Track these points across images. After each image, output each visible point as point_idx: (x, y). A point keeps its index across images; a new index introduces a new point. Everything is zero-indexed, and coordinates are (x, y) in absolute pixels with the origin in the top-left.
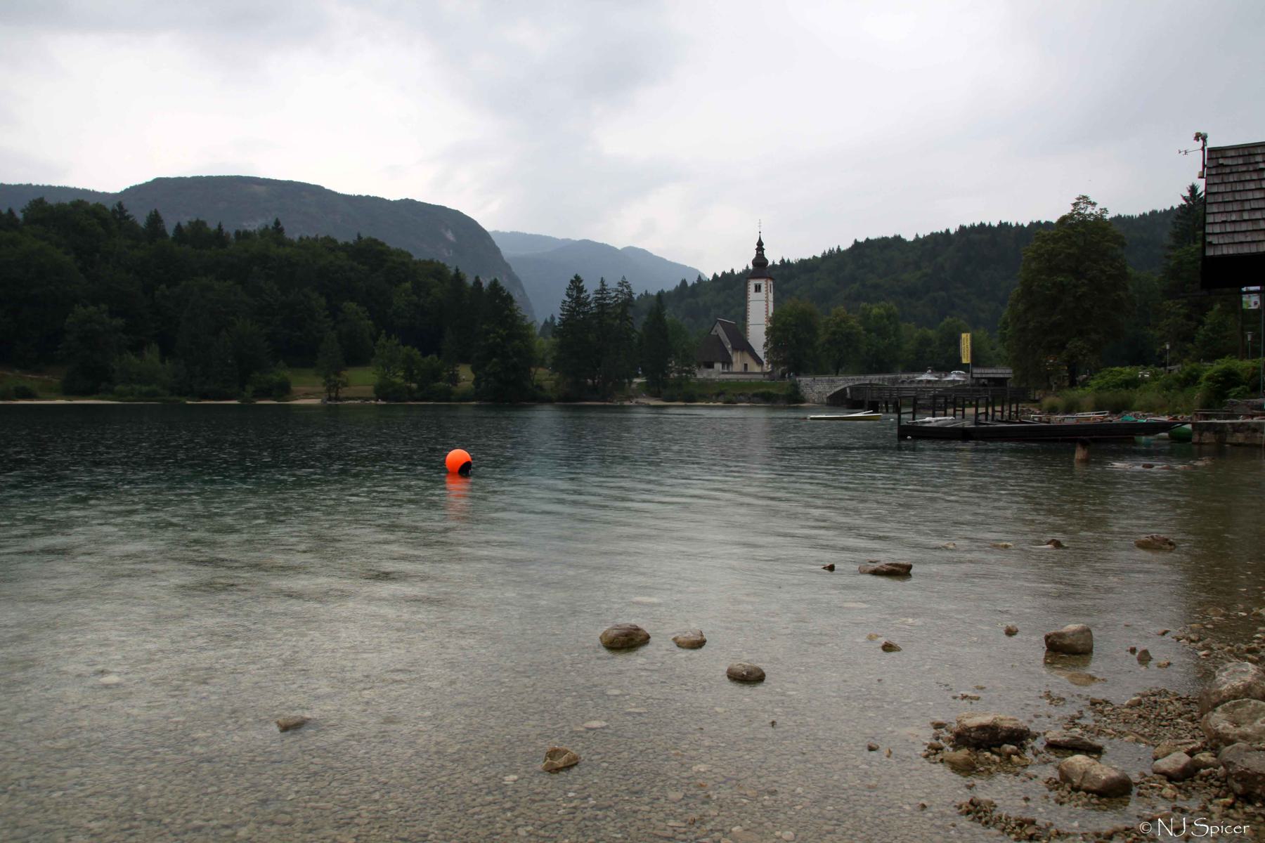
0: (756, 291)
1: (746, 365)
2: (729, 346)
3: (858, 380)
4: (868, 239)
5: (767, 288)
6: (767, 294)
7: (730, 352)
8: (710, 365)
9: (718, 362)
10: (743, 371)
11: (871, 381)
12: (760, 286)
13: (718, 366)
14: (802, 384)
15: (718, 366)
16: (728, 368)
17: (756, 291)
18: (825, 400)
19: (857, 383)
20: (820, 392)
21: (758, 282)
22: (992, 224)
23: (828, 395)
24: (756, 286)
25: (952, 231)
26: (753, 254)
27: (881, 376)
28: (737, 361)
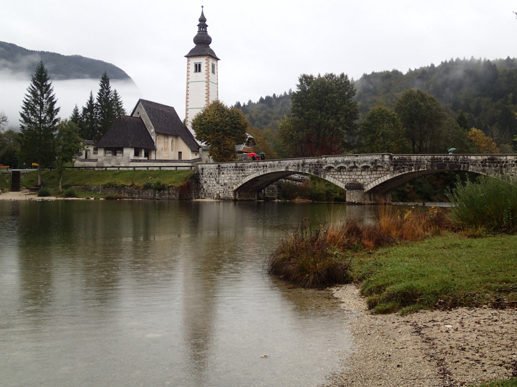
0: (196, 71)
1: (180, 153)
2: (152, 130)
3: (271, 166)
4: (373, 73)
5: (207, 67)
6: (208, 74)
7: (153, 137)
8: (116, 150)
9: (128, 147)
10: (177, 159)
11: (287, 168)
12: (200, 65)
13: (129, 153)
14: (206, 172)
15: (129, 153)
16: (147, 155)
17: (196, 71)
18: (232, 195)
19: (269, 171)
20: (225, 184)
21: (197, 60)
22: (466, 58)
23: (235, 187)
24: (196, 65)
25: (436, 65)
26: (195, 31)
27: (301, 161)
28: (166, 149)
